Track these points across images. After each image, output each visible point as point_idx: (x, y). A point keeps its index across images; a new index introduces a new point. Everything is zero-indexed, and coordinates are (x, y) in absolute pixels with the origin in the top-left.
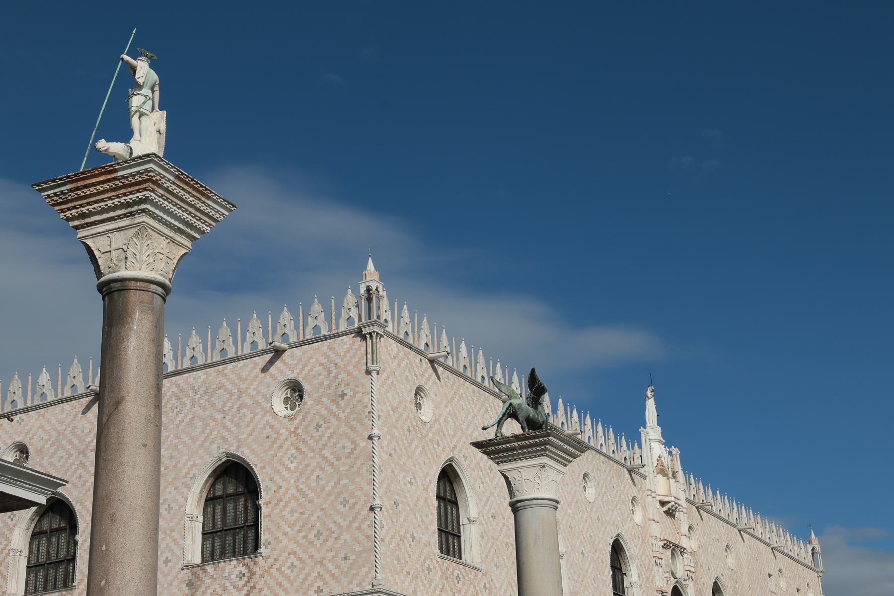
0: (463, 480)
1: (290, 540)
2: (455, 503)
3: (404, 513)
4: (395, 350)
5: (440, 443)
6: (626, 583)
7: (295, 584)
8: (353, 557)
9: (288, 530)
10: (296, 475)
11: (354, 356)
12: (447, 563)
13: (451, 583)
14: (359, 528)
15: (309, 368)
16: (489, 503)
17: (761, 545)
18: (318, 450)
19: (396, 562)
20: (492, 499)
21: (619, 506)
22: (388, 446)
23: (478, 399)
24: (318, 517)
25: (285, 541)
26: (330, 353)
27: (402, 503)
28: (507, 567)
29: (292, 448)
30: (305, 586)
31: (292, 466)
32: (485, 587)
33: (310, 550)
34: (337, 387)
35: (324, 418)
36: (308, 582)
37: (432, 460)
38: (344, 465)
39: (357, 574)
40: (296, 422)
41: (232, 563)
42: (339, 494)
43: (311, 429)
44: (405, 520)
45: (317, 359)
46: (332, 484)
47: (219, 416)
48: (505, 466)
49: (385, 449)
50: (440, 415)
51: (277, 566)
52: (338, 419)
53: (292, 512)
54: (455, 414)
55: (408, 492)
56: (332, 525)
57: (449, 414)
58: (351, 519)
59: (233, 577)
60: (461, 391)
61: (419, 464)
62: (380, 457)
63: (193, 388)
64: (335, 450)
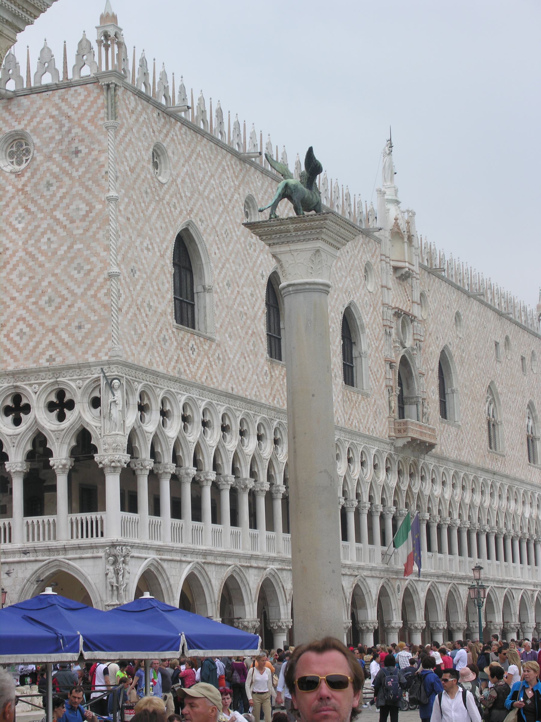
0: (199, 246)
1: (19, 305)
2: (190, 271)
3: (141, 281)
4: (133, 104)
5: (177, 205)
6: (355, 353)
7: (25, 352)
9: (16, 295)
10: (24, 236)
11: (88, 109)
12: (181, 334)
13: (186, 354)
14: (95, 296)
15: (38, 119)
16: (224, 270)
17: (490, 314)
18: (49, 211)
19: (133, 333)
20: (227, 265)
21: (352, 272)
22: (125, 209)
23: (216, 158)
25: (13, 306)
26: (64, 107)
27: (139, 270)
28: (240, 337)
29: (20, 207)
30: (36, 354)
31: (20, 226)
32: (219, 358)
33: (41, 317)
34: (70, 143)
35: (56, 177)
36: (39, 350)
37: (168, 225)
38: (78, 228)
39: (93, 344)
40: (24, 179)
42: (73, 259)
43: (42, 186)
44: (142, 288)
45: (47, 110)
46: (65, 248)
48: (277, 249)
49: (123, 213)
50: (178, 175)
52: (71, 178)
53: (21, 275)
54: (192, 174)
55: (145, 258)
56: (65, 292)
57: (187, 173)
58: (85, 286)
60: (199, 148)
61: (156, 229)
62: (117, 221)
64: (68, 211)
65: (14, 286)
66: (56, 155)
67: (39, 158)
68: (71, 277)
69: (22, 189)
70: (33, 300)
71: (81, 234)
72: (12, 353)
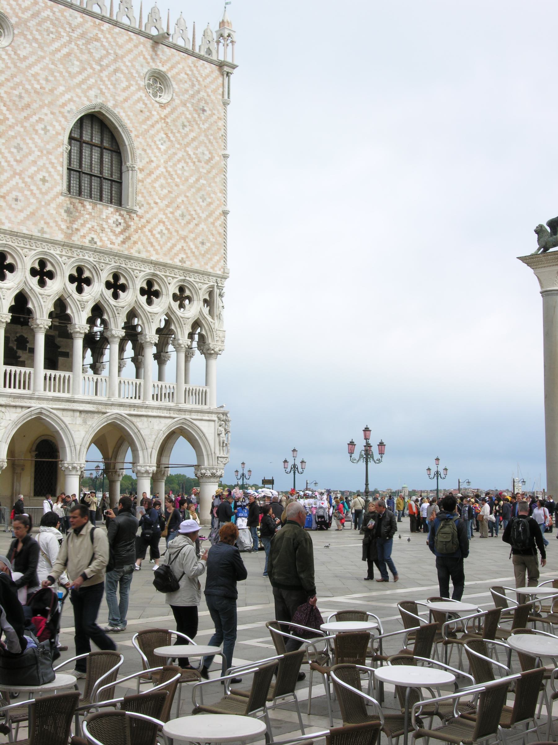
1: (160, 210)
8: (208, 245)
9: (158, 201)
10: (166, 157)
14: (213, 224)
24: (183, 201)
25: (156, 209)
29: (162, 132)
31: (163, 148)
38: (203, 168)
39: (211, 259)
41: (109, 208)
43: (179, 123)
47: (98, 68)
51: (149, 227)
53: (162, 187)
56: (193, 213)
58: (207, 213)
59: (111, 221)
63: (70, 24)
65: (157, 193)
66: (189, 105)
67: (177, 101)
68: (198, 203)
69: (164, 119)
70: (170, 210)
71: (205, 173)
72: (154, 246)
